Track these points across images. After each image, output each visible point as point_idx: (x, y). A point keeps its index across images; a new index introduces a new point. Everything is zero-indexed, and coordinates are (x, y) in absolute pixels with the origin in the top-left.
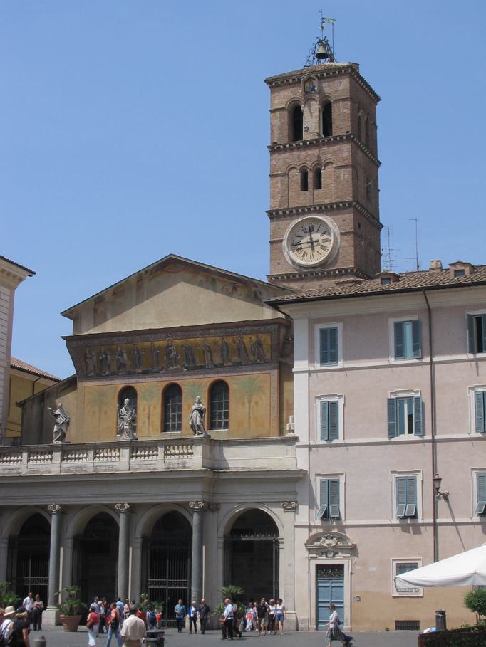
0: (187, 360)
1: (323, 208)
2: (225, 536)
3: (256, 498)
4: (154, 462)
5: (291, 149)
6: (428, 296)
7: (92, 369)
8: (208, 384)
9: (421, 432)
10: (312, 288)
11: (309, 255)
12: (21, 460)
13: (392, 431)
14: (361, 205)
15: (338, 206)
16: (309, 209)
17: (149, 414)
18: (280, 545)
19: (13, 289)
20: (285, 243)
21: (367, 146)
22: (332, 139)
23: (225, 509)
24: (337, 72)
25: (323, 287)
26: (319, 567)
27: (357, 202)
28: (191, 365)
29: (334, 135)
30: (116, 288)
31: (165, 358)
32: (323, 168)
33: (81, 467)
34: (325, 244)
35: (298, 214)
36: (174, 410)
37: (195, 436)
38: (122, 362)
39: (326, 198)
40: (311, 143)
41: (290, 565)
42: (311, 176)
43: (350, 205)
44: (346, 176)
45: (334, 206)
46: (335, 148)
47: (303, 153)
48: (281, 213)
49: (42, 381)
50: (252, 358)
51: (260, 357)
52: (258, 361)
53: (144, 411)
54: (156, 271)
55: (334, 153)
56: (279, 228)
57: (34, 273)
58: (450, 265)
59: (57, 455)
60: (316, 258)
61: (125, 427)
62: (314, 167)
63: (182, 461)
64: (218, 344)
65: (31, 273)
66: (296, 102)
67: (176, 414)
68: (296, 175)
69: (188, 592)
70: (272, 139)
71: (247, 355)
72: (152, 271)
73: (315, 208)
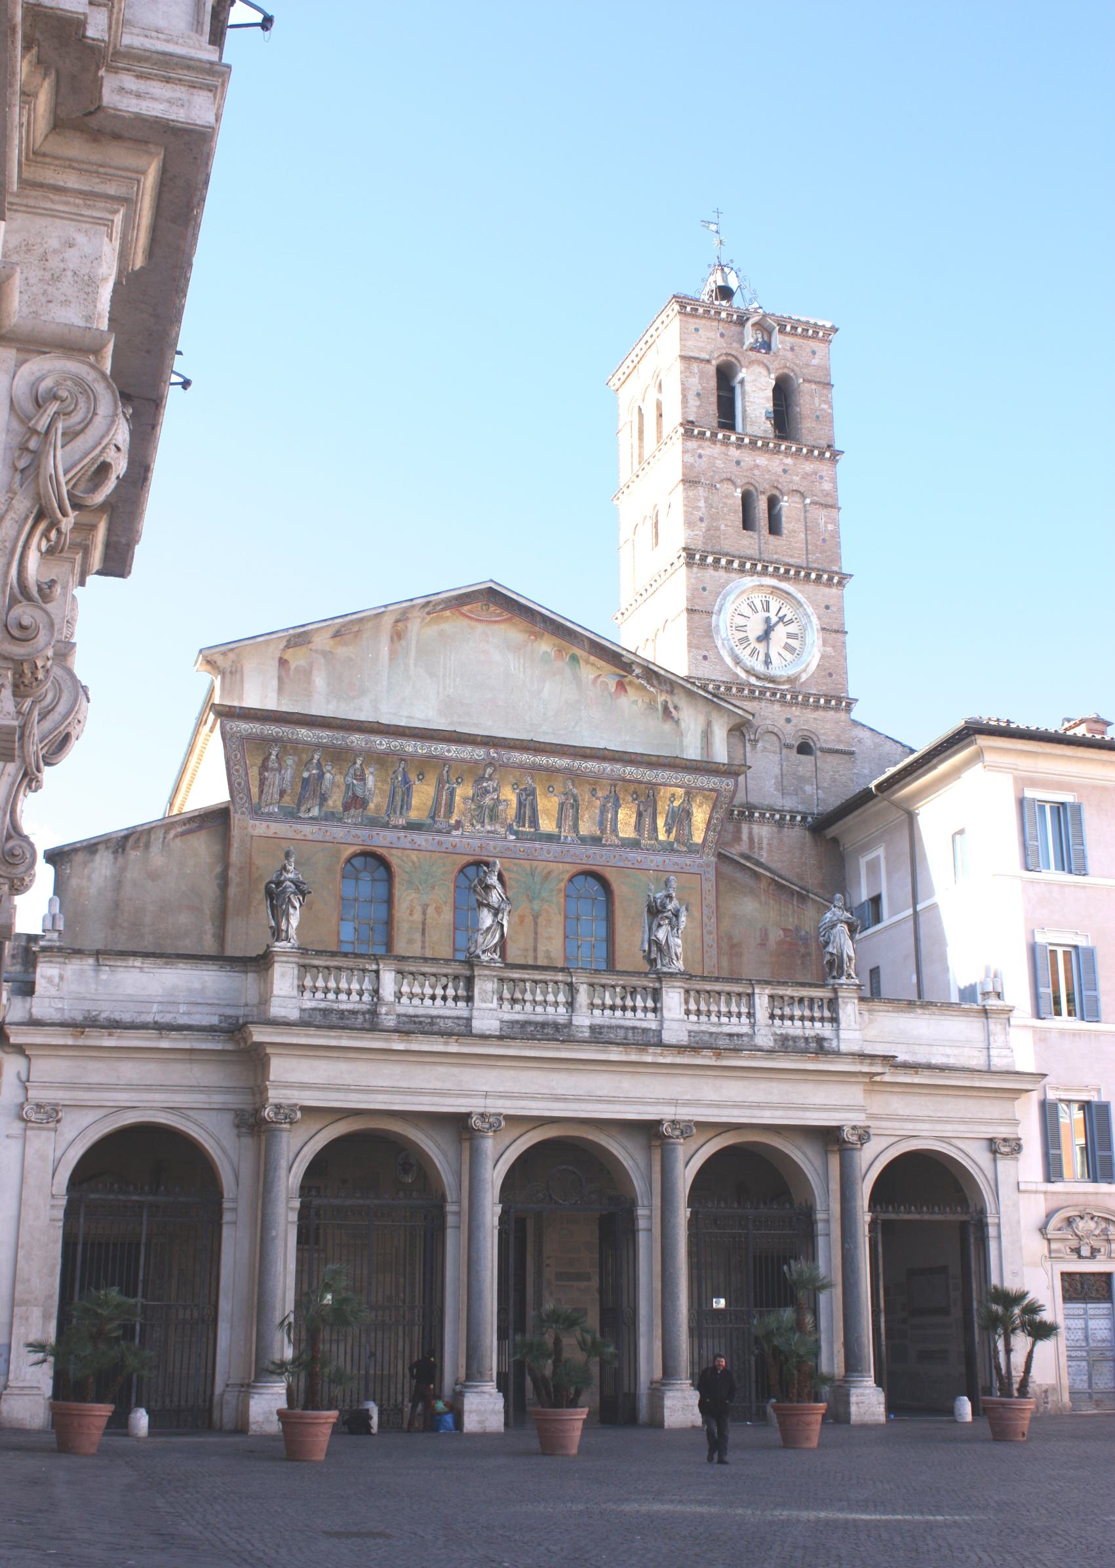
0: (520, 818)
1: (792, 572)
3: (939, 1127)
4: (745, 1029)
7: (276, 796)
8: (567, 876)
12: (376, 992)
16: (765, 568)
17: (424, 923)
22: (805, 451)
25: (794, 721)
26: (1068, 1278)
28: (526, 829)
30: (351, 622)
32: (786, 498)
33: (556, 1026)
38: (359, 793)
39: (792, 556)
40: (766, 445)
42: (761, 507)
44: (830, 527)
45: (813, 576)
46: (809, 467)
48: (710, 560)
51: (684, 839)
52: (675, 846)
53: (411, 914)
54: (443, 610)
55: (806, 476)
56: (704, 589)
63: (812, 1033)
64: (600, 794)
66: (733, 360)
70: (684, 413)
71: (655, 829)
72: (434, 606)
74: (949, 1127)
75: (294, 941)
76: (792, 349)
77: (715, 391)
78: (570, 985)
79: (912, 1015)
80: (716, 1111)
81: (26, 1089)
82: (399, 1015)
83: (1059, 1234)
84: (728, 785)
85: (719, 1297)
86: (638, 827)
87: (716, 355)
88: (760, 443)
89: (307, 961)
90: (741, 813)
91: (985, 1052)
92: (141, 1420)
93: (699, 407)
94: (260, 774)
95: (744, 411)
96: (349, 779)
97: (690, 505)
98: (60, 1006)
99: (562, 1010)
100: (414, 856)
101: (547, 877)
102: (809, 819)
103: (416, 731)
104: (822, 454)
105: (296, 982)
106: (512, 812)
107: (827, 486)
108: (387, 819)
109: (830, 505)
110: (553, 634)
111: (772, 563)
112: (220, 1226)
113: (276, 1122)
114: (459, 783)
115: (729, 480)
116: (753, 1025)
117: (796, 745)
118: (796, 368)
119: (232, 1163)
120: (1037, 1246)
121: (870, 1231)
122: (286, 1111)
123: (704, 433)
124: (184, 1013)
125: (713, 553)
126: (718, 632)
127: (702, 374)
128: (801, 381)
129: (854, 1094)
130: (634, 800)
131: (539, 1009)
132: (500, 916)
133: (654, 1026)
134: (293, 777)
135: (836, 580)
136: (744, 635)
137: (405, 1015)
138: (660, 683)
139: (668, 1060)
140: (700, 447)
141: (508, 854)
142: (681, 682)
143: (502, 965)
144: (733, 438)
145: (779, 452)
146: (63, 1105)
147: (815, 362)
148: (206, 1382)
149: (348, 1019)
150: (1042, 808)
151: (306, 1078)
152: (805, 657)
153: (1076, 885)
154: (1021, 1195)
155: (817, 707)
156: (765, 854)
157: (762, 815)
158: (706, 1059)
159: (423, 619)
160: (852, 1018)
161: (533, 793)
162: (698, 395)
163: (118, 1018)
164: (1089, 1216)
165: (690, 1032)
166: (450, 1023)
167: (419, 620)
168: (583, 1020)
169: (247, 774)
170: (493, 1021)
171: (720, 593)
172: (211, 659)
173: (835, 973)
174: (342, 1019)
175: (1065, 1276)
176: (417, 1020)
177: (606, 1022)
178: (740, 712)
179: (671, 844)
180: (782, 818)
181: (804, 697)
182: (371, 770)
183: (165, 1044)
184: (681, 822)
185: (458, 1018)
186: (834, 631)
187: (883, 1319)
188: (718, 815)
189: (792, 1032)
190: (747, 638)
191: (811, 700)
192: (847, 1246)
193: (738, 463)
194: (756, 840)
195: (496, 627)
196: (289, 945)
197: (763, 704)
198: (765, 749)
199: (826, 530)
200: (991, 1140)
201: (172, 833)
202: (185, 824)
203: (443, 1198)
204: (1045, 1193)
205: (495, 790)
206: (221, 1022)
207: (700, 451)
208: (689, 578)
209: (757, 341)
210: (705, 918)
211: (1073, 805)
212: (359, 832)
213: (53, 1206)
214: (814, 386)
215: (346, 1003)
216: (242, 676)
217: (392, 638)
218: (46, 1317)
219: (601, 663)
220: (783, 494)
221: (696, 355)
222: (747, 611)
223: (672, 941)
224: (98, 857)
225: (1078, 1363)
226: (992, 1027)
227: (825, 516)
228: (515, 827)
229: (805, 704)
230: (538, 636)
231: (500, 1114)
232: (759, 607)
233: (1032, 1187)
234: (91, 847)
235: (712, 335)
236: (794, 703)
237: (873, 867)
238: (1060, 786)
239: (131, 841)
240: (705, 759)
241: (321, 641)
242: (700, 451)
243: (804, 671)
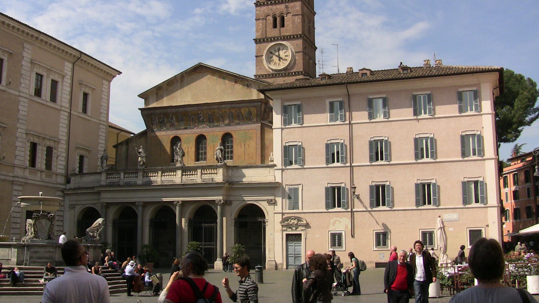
1: (285, 37)
2: (235, 219)
4: (195, 178)
5: (267, 4)
6: (348, 87)
8: (221, 135)
10: (280, 81)
11: (277, 64)
12: (120, 177)
13: (464, 154)
14: (306, 37)
15: (294, 37)
16: (278, 38)
18: (266, 223)
19: (110, 81)
20: (264, 57)
21: (309, 4)
23: (235, 204)
27: (305, 35)
35: (271, 41)
36: (202, 150)
37: (218, 164)
39: (287, 33)
41: (271, 234)
43: (300, 36)
44: (298, 21)
45: (292, 37)
49: (123, 133)
52: (249, 122)
54: (192, 72)
56: (261, 49)
57: (121, 73)
58: (359, 70)
59: (140, 174)
60: (283, 65)
61: (179, 159)
62: (280, 15)
63: (211, 178)
65: (120, 73)
67: (203, 151)
68: (270, 19)
69: (215, 250)
72: (189, 72)
75: (105, 169)
96: (170, 120)
97: (257, 26)
100: (186, 135)
101: (217, 136)
120: (279, 227)
133: (174, 179)
140: (260, 8)
141: (207, 131)
144: (269, 3)
172: (141, 96)
177: (165, 180)
182: (174, 117)
184: (249, 116)
189: (206, 178)
191: (290, 74)
193: (271, 9)
197: (277, 78)
201: (137, 138)
207: (261, 9)
208: (256, 47)
212: (173, 132)
215: (115, 180)
219: (231, 77)
227: (297, 18)
238: (296, 100)
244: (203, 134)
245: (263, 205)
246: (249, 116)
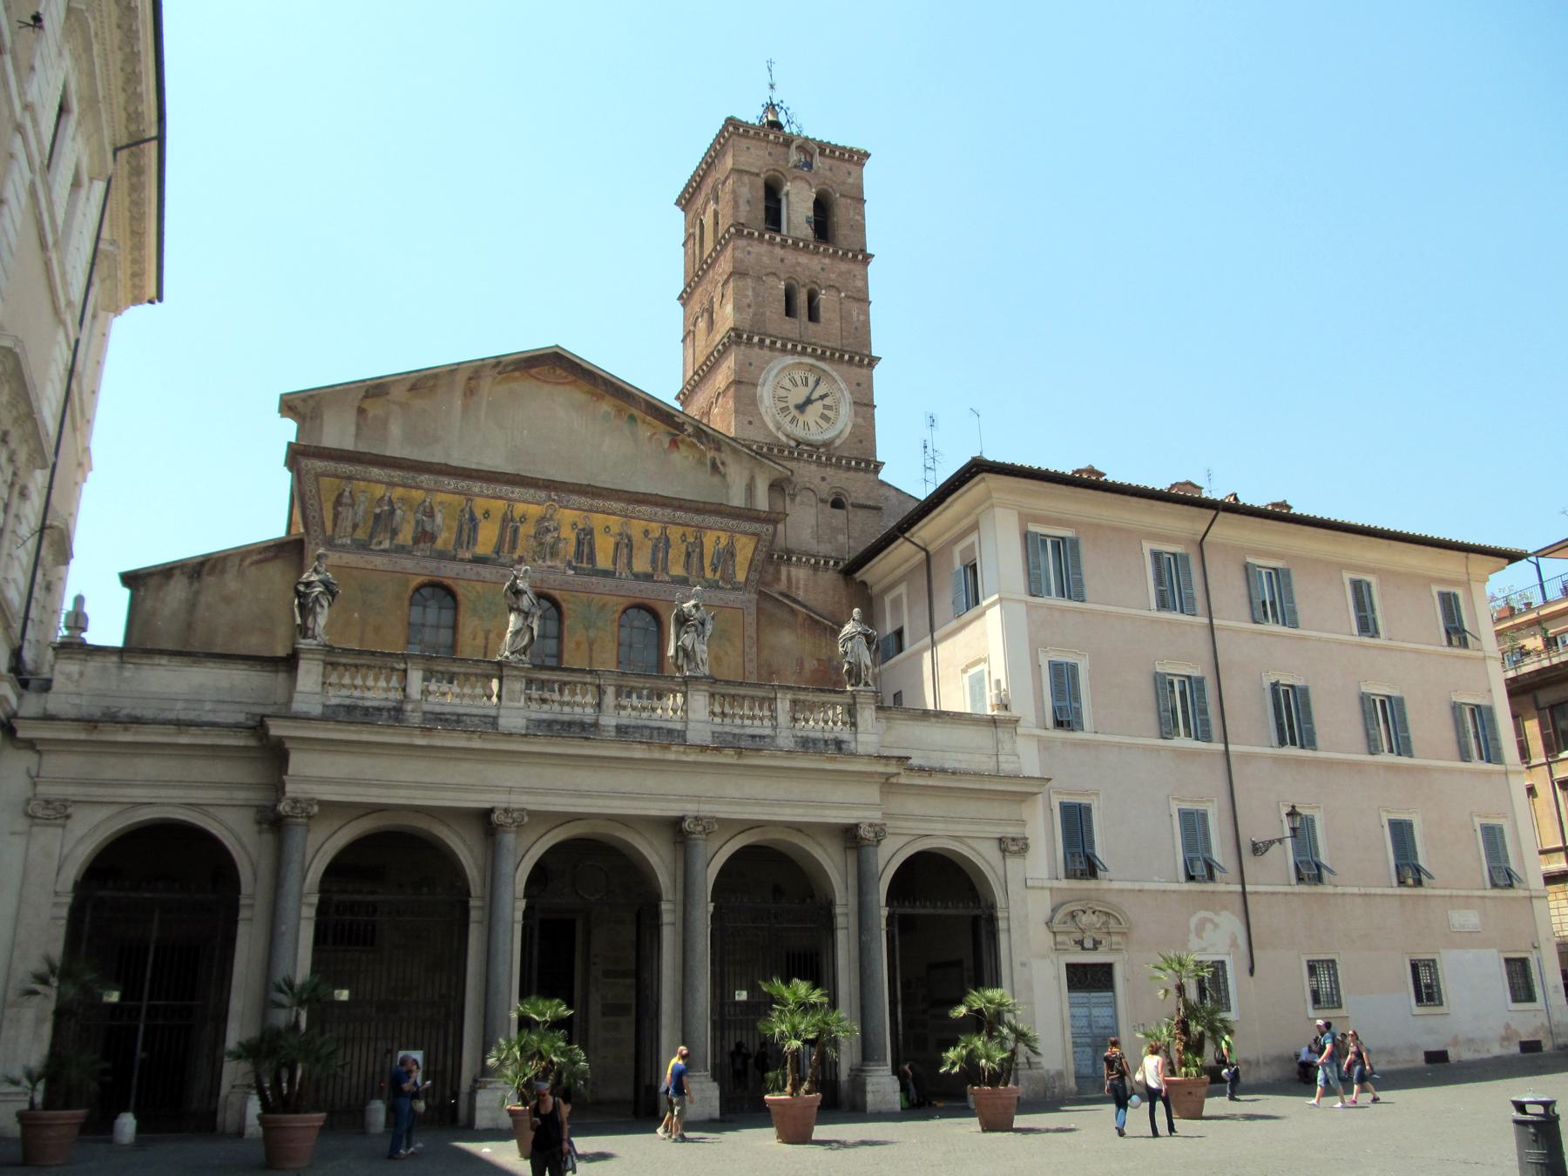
0: (579, 555)
1: (828, 353)
3: (951, 826)
4: (768, 732)
7: (349, 530)
8: (621, 608)
9: (1207, 737)
16: (804, 349)
17: (486, 647)
22: (840, 253)
24: (847, 156)
25: (829, 480)
26: (1071, 968)
28: (584, 565)
29: (845, 245)
30: (426, 376)
31: (533, 543)
32: (823, 292)
33: (583, 726)
34: (826, 412)
38: (428, 528)
39: (828, 341)
40: (806, 246)
41: (1023, 965)
42: (802, 299)
44: (862, 318)
45: (847, 357)
46: (844, 267)
47: (791, 257)
48: (756, 339)
50: (709, 574)
51: (728, 578)
53: (474, 639)
54: (513, 370)
55: (840, 274)
56: (750, 364)
63: (831, 736)
71: (702, 568)
72: (508, 365)
73: (814, 350)
74: (961, 827)
76: (831, 169)
77: (763, 200)
78: (599, 686)
79: (923, 723)
80: (738, 809)
81: (35, 785)
82: (425, 713)
83: (1062, 928)
84: (767, 530)
85: (741, 989)
86: (687, 565)
87: (764, 170)
88: (801, 244)
89: (334, 659)
90: (781, 557)
91: (994, 758)
92: (127, 1124)
93: (748, 212)
94: (335, 508)
95: (789, 218)
96: (419, 516)
98: (77, 701)
99: (589, 710)
100: (479, 586)
102: (841, 563)
103: (481, 474)
104: (855, 256)
105: (320, 679)
106: (572, 549)
107: (859, 284)
108: (454, 552)
109: (863, 300)
110: (613, 395)
111: (810, 344)
112: (235, 923)
113: (292, 817)
114: (522, 522)
115: (774, 274)
116: (775, 727)
117: (830, 500)
118: (834, 185)
119: (252, 864)
120: (1043, 938)
121: (887, 925)
122: (304, 805)
123: (753, 234)
124: (210, 711)
125: (758, 334)
126: (762, 402)
127: (752, 185)
128: (838, 195)
129: (872, 793)
130: (683, 541)
131: (567, 709)
132: (530, 619)
134: (366, 512)
135: (866, 362)
136: (784, 405)
137: (432, 713)
138: (709, 441)
139: (691, 758)
140: (749, 245)
142: (727, 440)
143: (530, 666)
144: (778, 239)
145: (818, 253)
146: (75, 802)
147: (850, 180)
148: (15, 1101)
149: (372, 715)
150: (1044, 543)
151: (327, 772)
152: (839, 426)
153: (1075, 610)
154: (1028, 891)
155: (849, 468)
156: (802, 594)
157: (799, 560)
158: (728, 757)
159: (495, 379)
160: (869, 721)
161: (589, 532)
162: (748, 202)
163: (139, 715)
164: (1091, 911)
165: (713, 733)
166: (476, 720)
167: (490, 379)
168: (609, 720)
169: (321, 509)
170: (520, 720)
171: (764, 368)
172: (291, 405)
173: (853, 681)
174: (367, 715)
175: (1069, 966)
176: (442, 717)
177: (633, 722)
178: (780, 468)
179: (717, 582)
180: (817, 563)
181: (837, 459)
183: (184, 740)
184: (725, 561)
185: (485, 716)
186: (865, 405)
187: (899, 1010)
188: (761, 556)
190: (787, 408)
191: (844, 462)
192: (864, 939)
194: (794, 581)
195: (561, 388)
196: (315, 642)
197: (801, 464)
198: (802, 503)
199: (858, 320)
200: (1000, 840)
201: (248, 561)
202: (260, 553)
203: (468, 894)
204: (1051, 889)
205: (555, 529)
206: (247, 719)
207: (749, 248)
209: (800, 161)
210: (747, 649)
211: (1071, 540)
212: (428, 565)
213: (55, 905)
214: (849, 201)
216: (322, 420)
217: (465, 395)
218: (39, 1021)
220: (821, 289)
221: (747, 169)
222: (787, 384)
223: (697, 649)
224: (172, 582)
225: (1083, 1049)
226: (1000, 734)
228: (574, 564)
229: (838, 465)
230: (600, 397)
231: (523, 810)
232: (799, 382)
233: (1038, 883)
234: (166, 572)
235: (761, 153)
236: (828, 464)
237: (896, 604)
239: (207, 568)
240: (749, 506)
241: (398, 393)
242: (749, 248)
243: (838, 436)
244: (552, 592)
245: (983, 856)
246: (725, 561)
